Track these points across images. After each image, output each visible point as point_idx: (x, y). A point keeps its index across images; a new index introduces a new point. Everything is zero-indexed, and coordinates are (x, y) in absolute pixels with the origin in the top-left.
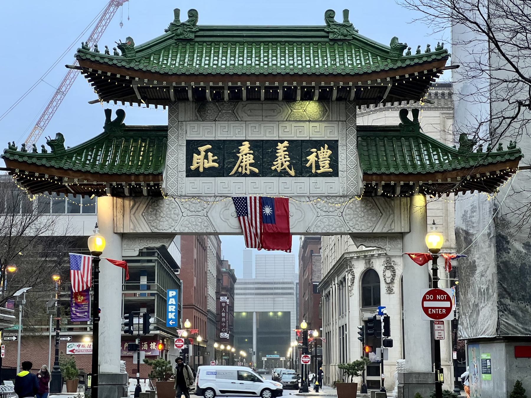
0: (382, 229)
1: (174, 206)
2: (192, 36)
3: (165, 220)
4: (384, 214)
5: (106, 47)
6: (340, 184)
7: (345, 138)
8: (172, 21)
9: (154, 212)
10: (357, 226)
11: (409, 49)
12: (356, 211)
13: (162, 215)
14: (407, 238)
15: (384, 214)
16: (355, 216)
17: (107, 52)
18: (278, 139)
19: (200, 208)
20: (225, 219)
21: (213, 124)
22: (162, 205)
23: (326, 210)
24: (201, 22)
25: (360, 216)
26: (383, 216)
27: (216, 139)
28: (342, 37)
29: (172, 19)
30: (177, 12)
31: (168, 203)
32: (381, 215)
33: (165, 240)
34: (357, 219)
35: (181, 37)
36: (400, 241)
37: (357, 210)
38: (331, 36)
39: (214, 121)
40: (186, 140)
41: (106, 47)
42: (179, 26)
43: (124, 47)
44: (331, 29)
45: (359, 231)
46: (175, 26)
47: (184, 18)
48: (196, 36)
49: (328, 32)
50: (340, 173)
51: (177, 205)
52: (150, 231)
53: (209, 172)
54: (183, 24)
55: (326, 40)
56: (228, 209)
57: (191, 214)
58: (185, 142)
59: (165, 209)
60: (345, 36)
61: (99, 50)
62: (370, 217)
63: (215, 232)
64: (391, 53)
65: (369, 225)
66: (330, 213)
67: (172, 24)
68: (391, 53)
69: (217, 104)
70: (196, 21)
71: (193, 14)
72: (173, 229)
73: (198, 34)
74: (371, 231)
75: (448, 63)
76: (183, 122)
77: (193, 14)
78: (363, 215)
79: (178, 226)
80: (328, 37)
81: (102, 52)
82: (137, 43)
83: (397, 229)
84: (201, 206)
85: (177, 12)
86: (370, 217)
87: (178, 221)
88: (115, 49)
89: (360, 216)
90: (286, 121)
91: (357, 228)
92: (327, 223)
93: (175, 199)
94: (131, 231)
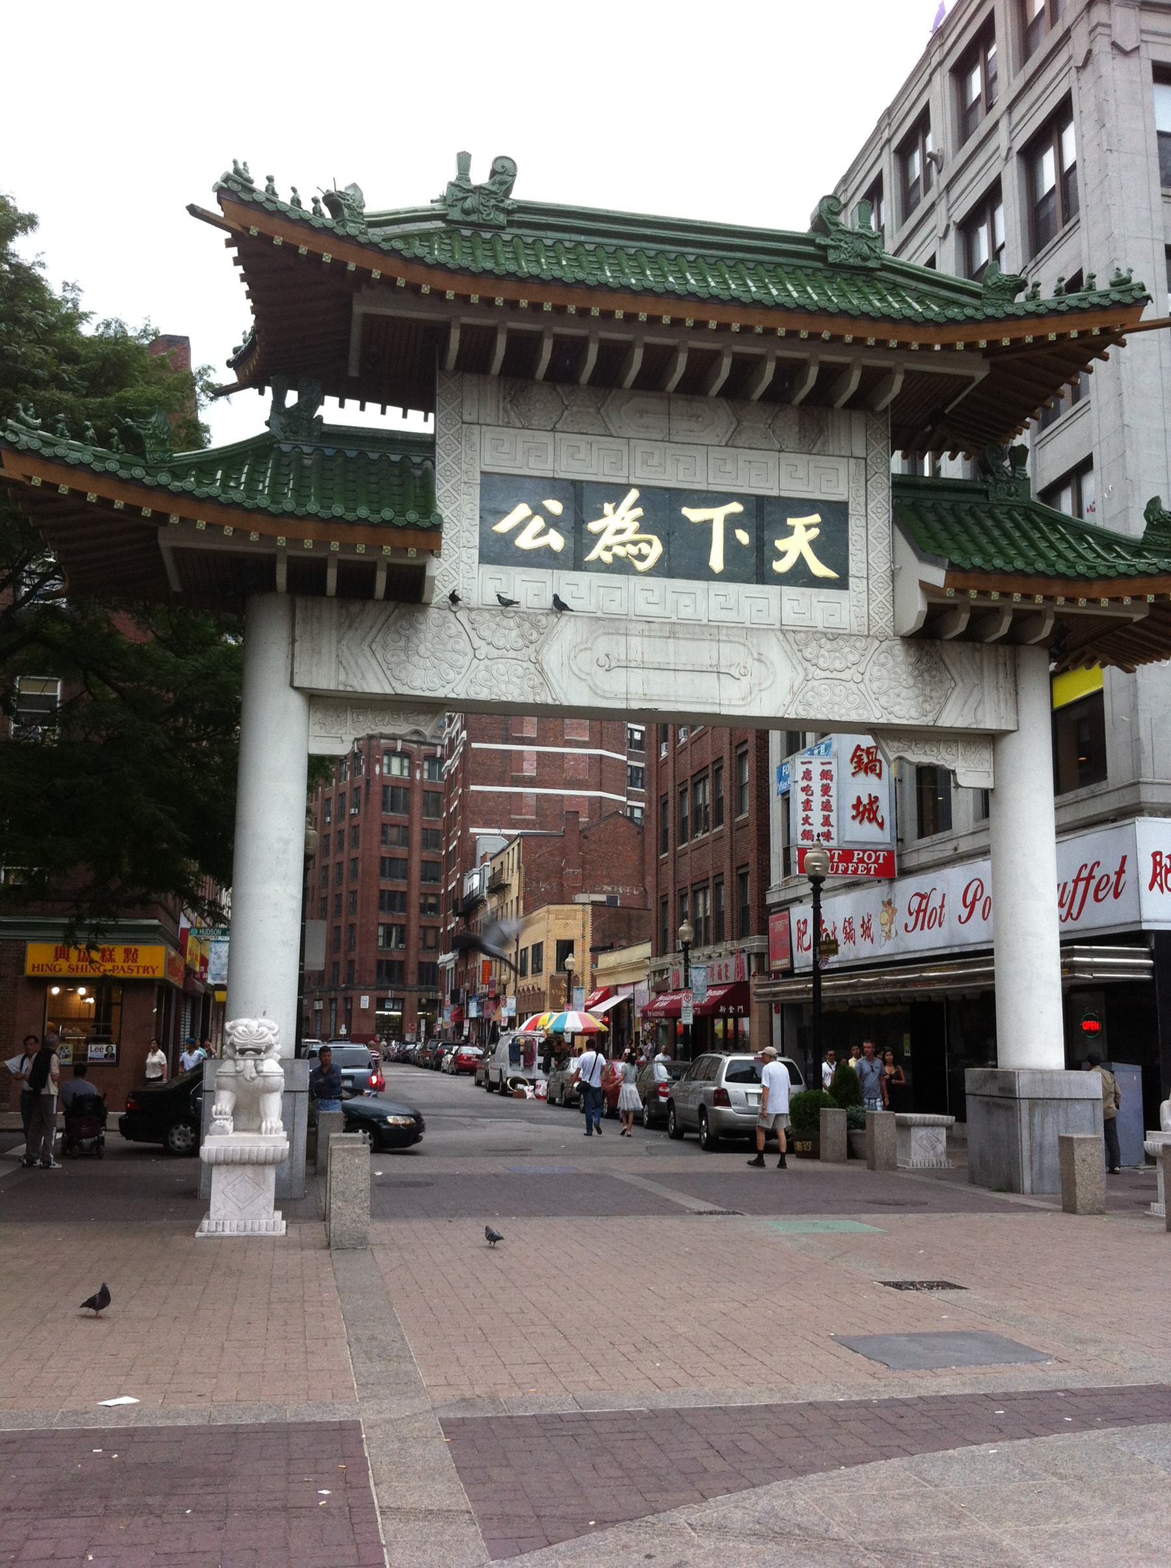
0: (956, 720)
1: (453, 631)
2: (502, 219)
3: (429, 664)
4: (960, 684)
5: (294, 190)
6: (853, 608)
7: (863, 498)
8: (453, 179)
9: (402, 643)
10: (897, 708)
11: (1037, 285)
12: (896, 673)
13: (422, 649)
14: (1010, 746)
15: (960, 684)
16: (893, 684)
17: (296, 202)
18: (705, 488)
19: (520, 640)
20: (580, 670)
21: (545, 437)
22: (423, 627)
23: (825, 665)
24: (522, 192)
25: (904, 683)
26: (958, 689)
27: (556, 476)
28: (858, 262)
29: (453, 176)
30: (464, 161)
31: (439, 622)
32: (953, 685)
33: (421, 718)
34: (896, 691)
35: (473, 218)
36: (986, 754)
37: (897, 670)
38: (832, 257)
39: (552, 430)
40: (482, 473)
41: (294, 190)
42: (469, 191)
43: (343, 202)
44: (832, 240)
45: (906, 722)
46: (460, 188)
47: (480, 176)
48: (511, 224)
49: (825, 248)
50: (851, 580)
51: (461, 629)
52: (389, 691)
53: (542, 558)
54: (479, 189)
55: (820, 265)
56: (591, 649)
57: (494, 653)
58: (478, 476)
59: (430, 636)
60: (865, 258)
61: (277, 191)
62: (928, 688)
63: (558, 703)
64: (988, 299)
65: (927, 707)
66: (835, 675)
67: (452, 185)
68: (988, 299)
69: (559, 389)
70: (509, 190)
71: (504, 172)
72: (449, 687)
73: (517, 217)
74: (931, 724)
75: (1149, 313)
76: (473, 426)
77: (504, 172)
78: (911, 682)
79: (463, 682)
80: (824, 259)
81: (285, 197)
82: (374, 205)
83: (990, 723)
84: (522, 636)
85: (464, 161)
86: (928, 688)
87: (463, 671)
88: (315, 201)
89: (904, 683)
90: (726, 445)
91: (901, 713)
92: (825, 699)
93: (455, 612)
94: (341, 688)
